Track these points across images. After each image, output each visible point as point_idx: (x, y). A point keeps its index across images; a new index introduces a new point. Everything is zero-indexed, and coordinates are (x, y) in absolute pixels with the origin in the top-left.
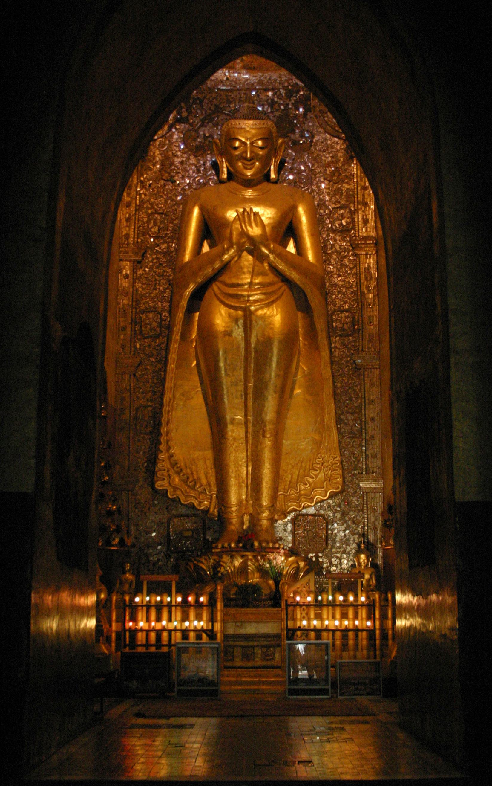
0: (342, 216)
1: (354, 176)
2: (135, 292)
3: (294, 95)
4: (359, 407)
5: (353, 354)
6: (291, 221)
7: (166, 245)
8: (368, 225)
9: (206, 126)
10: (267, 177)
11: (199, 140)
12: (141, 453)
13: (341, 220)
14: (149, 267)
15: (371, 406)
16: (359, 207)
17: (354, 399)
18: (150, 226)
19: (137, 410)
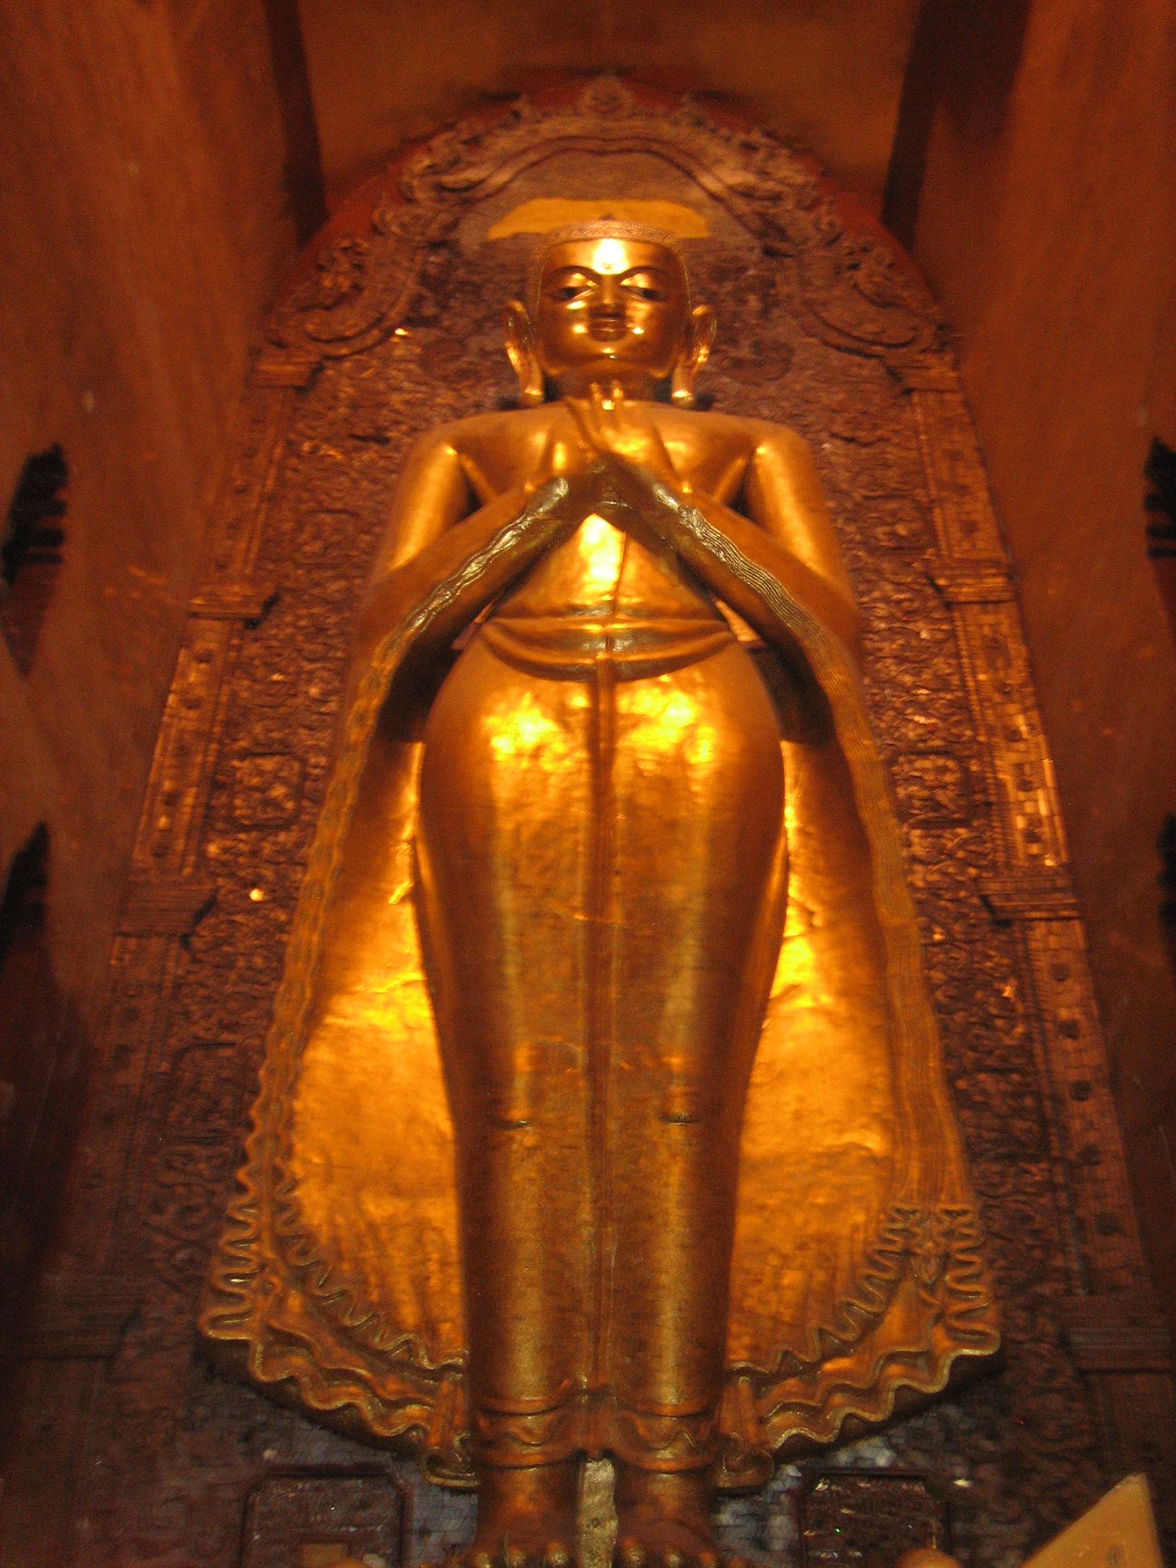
0: (896, 517)
4: (1025, 1048)
5: (975, 880)
8: (978, 535)
10: (662, 394)
12: (172, 1209)
15: (1069, 1044)
17: (999, 1023)
19: (178, 1056)
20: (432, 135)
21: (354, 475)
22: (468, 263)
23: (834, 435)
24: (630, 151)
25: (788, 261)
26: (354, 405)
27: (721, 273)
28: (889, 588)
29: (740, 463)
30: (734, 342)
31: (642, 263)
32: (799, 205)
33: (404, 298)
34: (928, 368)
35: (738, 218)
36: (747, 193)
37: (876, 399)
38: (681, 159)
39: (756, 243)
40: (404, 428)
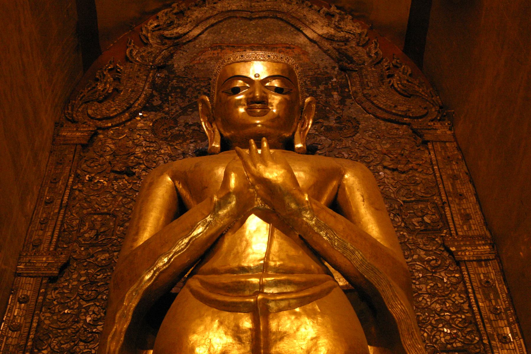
1: (432, 164)
2: (35, 325)
3: (324, 83)
6: (337, 195)
7: (107, 255)
9: (190, 115)
10: (288, 145)
11: (177, 128)
13: (422, 217)
14: (70, 287)
16: (450, 199)
18: (82, 231)
20: (159, 10)
21: (114, 193)
22: (179, 77)
23: (385, 167)
24: (266, 17)
25: (354, 74)
26: (114, 154)
27: (317, 81)
28: (422, 253)
29: (335, 183)
30: (327, 118)
31: (276, 73)
32: (358, 44)
33: (143, 96)
34: (436, 129)
35: (326, 52)
36: (330, 39)
37: (408, 147)
38: (293, 21)
39: (336, 65)
40: (143, 166)
